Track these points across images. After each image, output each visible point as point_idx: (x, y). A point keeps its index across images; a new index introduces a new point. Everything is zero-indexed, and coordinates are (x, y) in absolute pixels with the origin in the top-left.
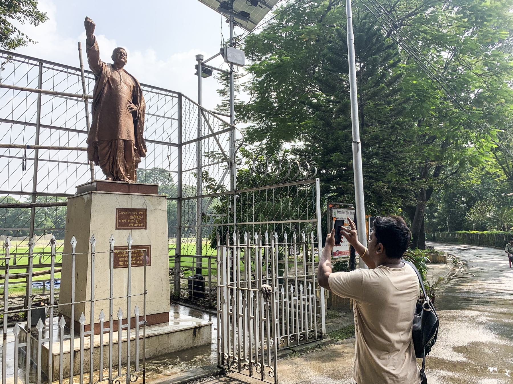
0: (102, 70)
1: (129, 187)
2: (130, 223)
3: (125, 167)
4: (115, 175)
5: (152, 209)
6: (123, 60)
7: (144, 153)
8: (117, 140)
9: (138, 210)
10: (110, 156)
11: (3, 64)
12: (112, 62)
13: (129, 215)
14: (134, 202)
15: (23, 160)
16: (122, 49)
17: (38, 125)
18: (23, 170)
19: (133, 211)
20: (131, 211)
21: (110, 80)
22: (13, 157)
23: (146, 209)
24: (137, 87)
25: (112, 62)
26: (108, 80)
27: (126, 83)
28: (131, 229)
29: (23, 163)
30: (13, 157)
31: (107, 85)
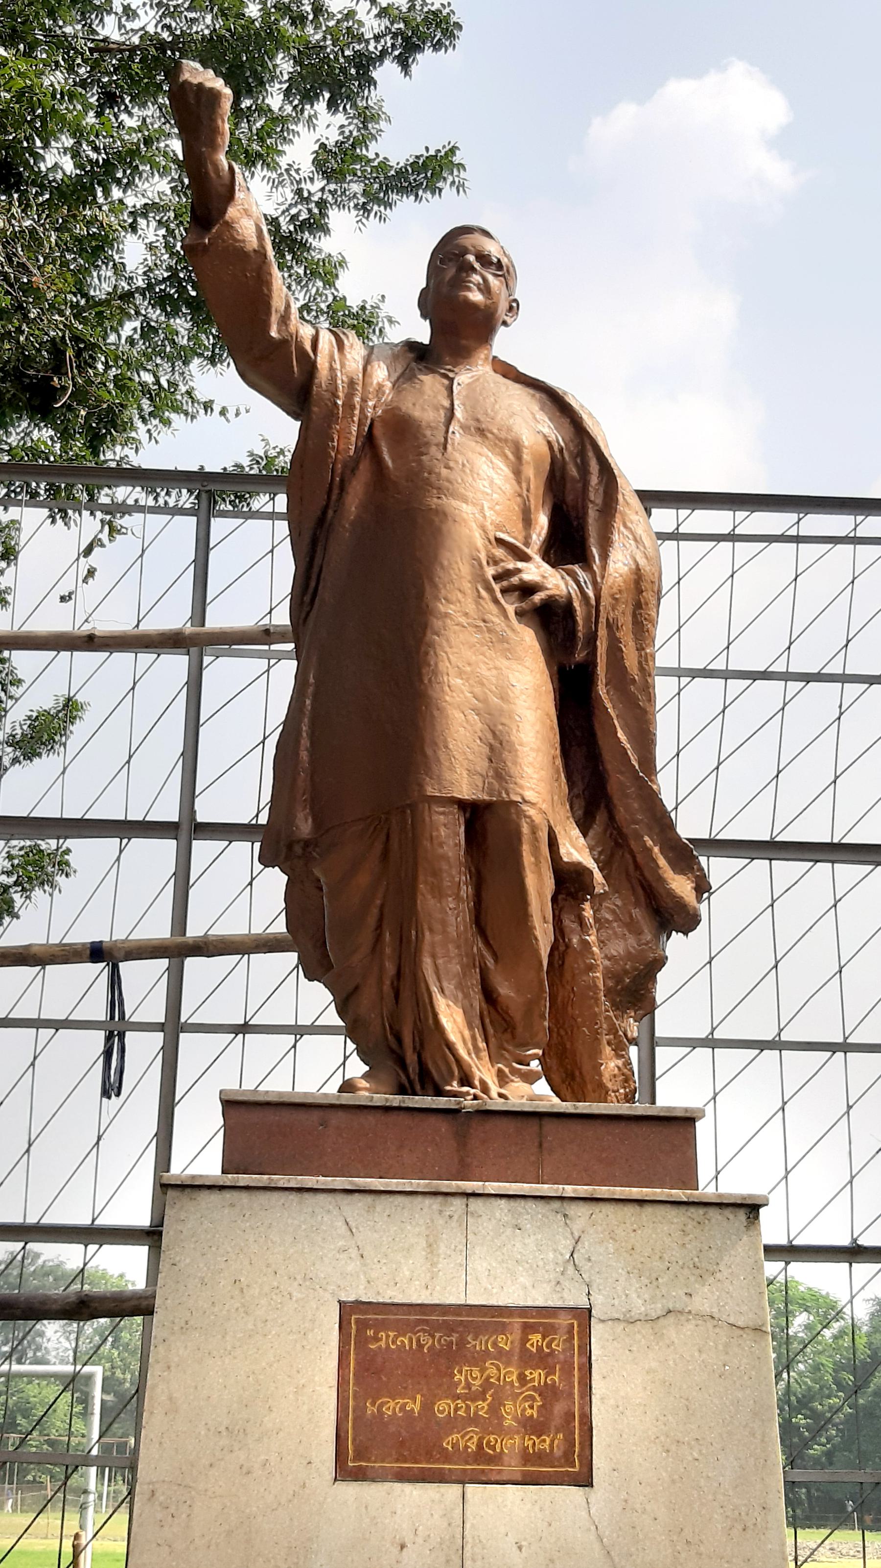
0: (310, 367)
1: (462, 1140)
2: (452, 1423)
3: (489, 995)
4: (411, 1058)
5: (639, 1307)
6: (476, 296)
7: (681, 905)
8: (413, 807)
9: (537, 1318)
10: (379, 927)
11: (88, 551)
12: (422, 333)
13: (455, 1355)
14: (490, 1254)
15: (109, 1038)
16: (466, 230)
17: (185, 827)
18: (106, 1093)
19: (478, 1330)
20: (457, 1329)
21: (378, 432)
22: (57, 1025)
23: (584, 1315)
24: (580, 455)
25: (422, 333)
26: (369, 440)
27: (481, 432)
28: (463, 1480)
29: (107, 1054)
30: (57, 1025)
31: (365, 468)
